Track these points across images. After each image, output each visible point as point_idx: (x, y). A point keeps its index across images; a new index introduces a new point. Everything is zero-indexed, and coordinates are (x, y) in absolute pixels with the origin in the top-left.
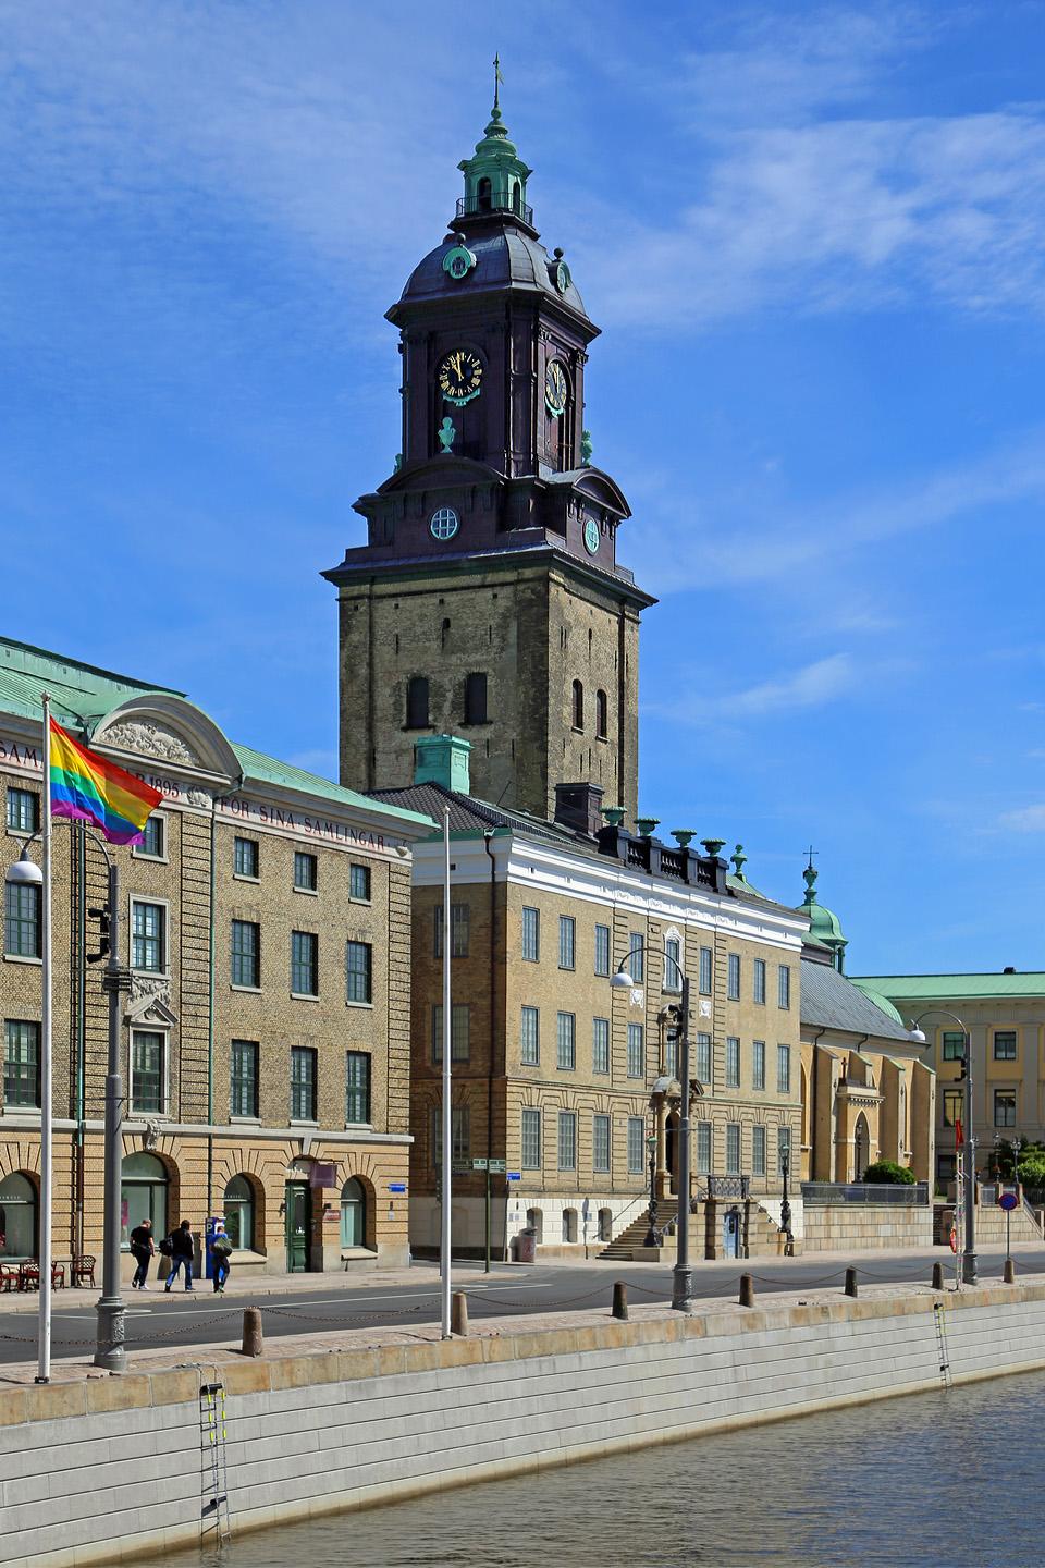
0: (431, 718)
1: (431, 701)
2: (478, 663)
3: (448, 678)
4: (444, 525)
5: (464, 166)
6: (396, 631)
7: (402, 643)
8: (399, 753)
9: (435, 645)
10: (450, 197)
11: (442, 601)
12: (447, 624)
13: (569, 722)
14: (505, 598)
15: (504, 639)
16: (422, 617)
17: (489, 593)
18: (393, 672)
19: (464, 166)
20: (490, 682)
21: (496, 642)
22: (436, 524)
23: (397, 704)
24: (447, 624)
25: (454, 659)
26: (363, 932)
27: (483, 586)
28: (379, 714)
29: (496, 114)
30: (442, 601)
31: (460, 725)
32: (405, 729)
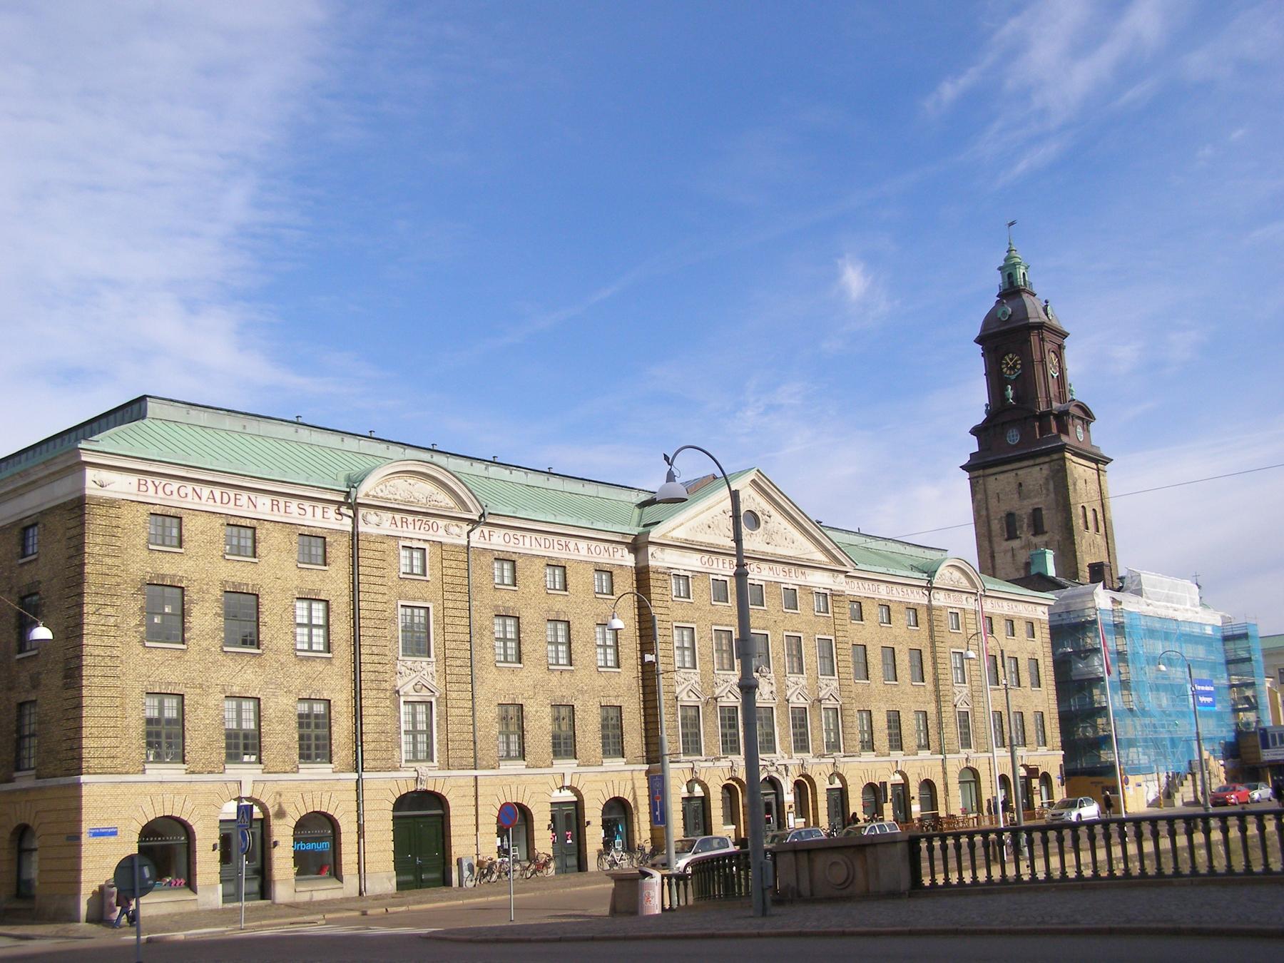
0: (1018, 533)
1: (1017, 524)
2: (1037, 503)
3: (1023, 510)
4: (1013, 437)
5: (1000, 269)
6: (998, 491)
7: (1001, 496)
8: (1005, 552)
9: (1016, 496)
10: (995, 282)
11: (1017, 474)
12: (1020, 485)
13: (1082, 528)
14: (1046, 470)
15: (1048, 490)
16: (1009, 483)
17: (1038, 468)
18: (998, 511)
19: (1000, 269)
21: (1044, 492)
22: (1009, 437)
24: (1020, 485)
25: (1025, 502)
26: (1034, 654)
28: (993, 534)
30: (1017, 474)
31: (1033, 535)
32: (1007, 540)
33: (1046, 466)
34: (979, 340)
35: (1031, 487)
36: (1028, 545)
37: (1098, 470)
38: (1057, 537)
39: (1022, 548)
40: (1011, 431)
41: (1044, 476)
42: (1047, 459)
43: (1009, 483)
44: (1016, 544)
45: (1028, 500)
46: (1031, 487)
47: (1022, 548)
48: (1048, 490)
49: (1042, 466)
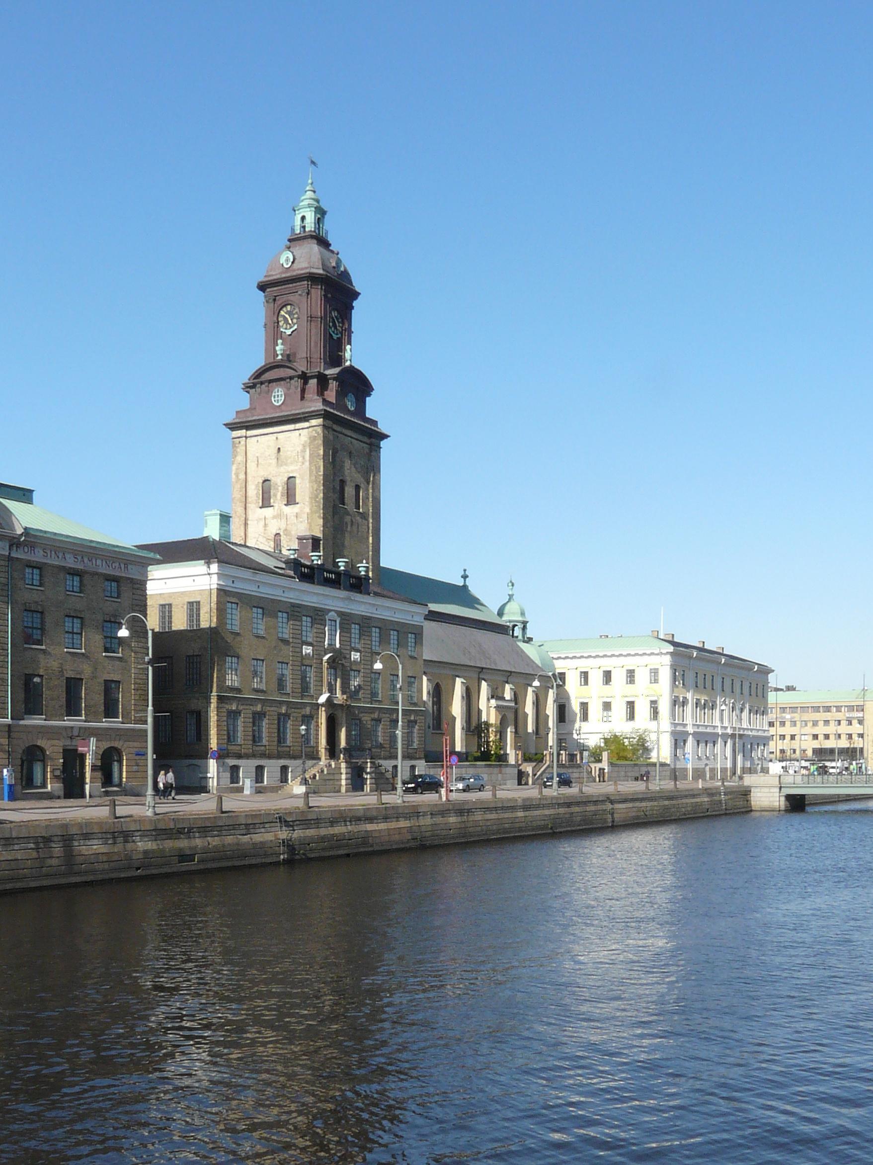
0: (272, 501)
2: (292, 471)
6: (257, 455)
8: (258, 520)
9: (274, 461)
11: (277, 438)
15: (304, 458)
16: (269, 446)
20: (298, 481)
21: (301, 459)
23: (257, 494)
25: (282, 469)
30: (277, 438)
32: (261, 508)
35: (289, 453)
36: (279, 516)
37: (370, 444)
38: (307, 510)
39: (274, 517)
40: (276, 390)
41: (302, 443)
42: (306, 424)
43: (269, 446)
44: (268, 512)
45: (285, 467)
46: (289, 453)
47: (274, 517)
48: (304, 458)
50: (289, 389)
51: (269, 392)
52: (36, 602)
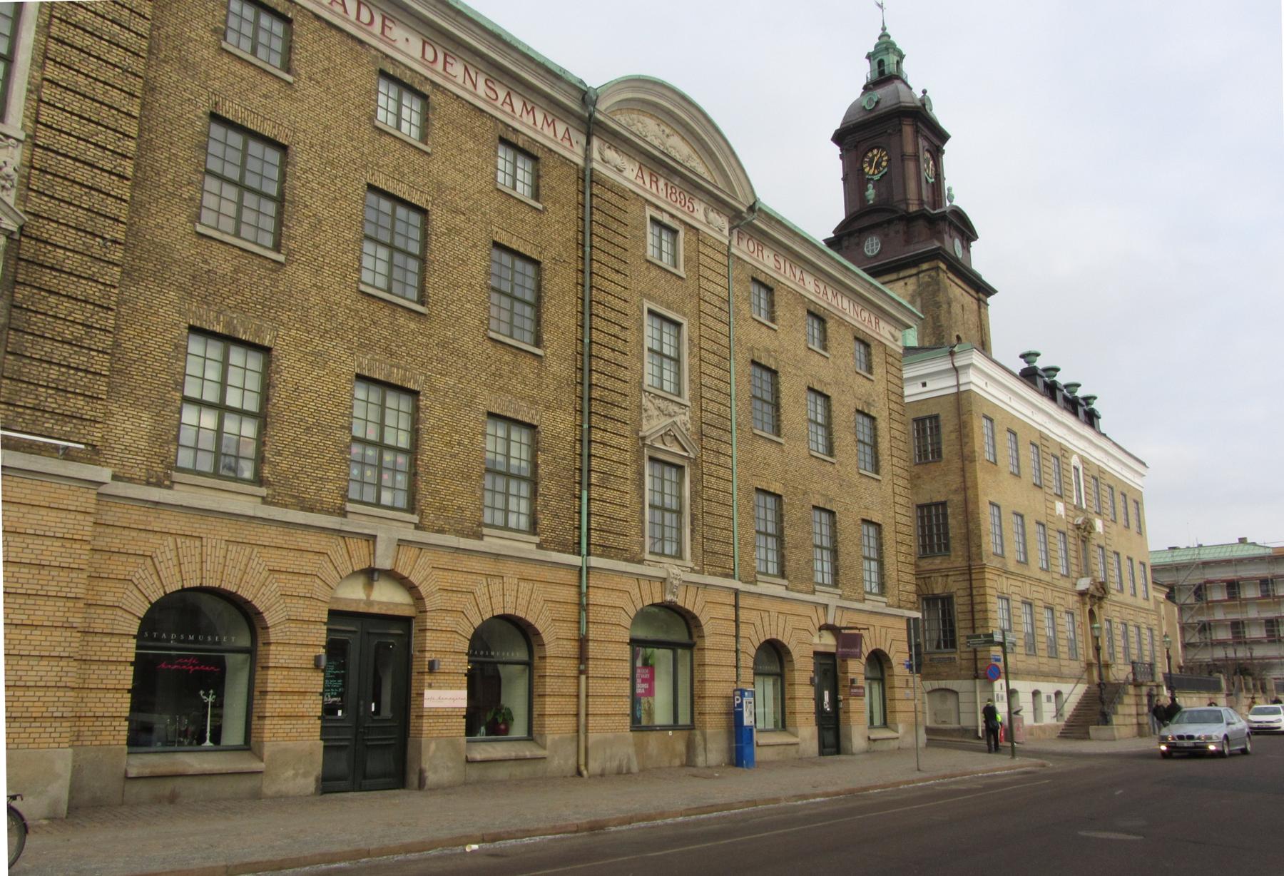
10: (863, 72)
17: (902, 283)
26: (868, 404)
27: (898, 279)
29: (884, 29)
33: (912, 281)
34: (839, 138)
37: (979, 300)
41: (910, 292)
42: (914, 271)
49: (906, 280)
50: (887, 235)
51: (860, 245)
52: (767, 351)
